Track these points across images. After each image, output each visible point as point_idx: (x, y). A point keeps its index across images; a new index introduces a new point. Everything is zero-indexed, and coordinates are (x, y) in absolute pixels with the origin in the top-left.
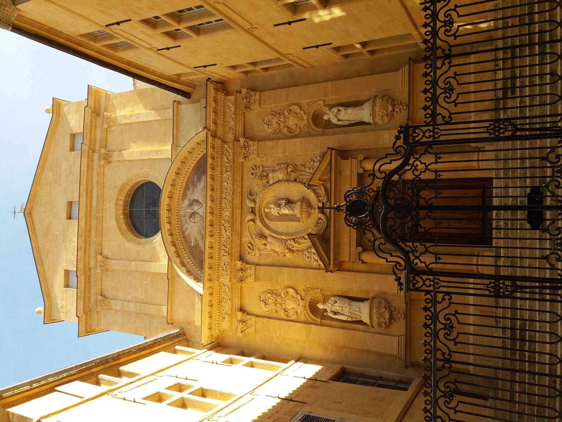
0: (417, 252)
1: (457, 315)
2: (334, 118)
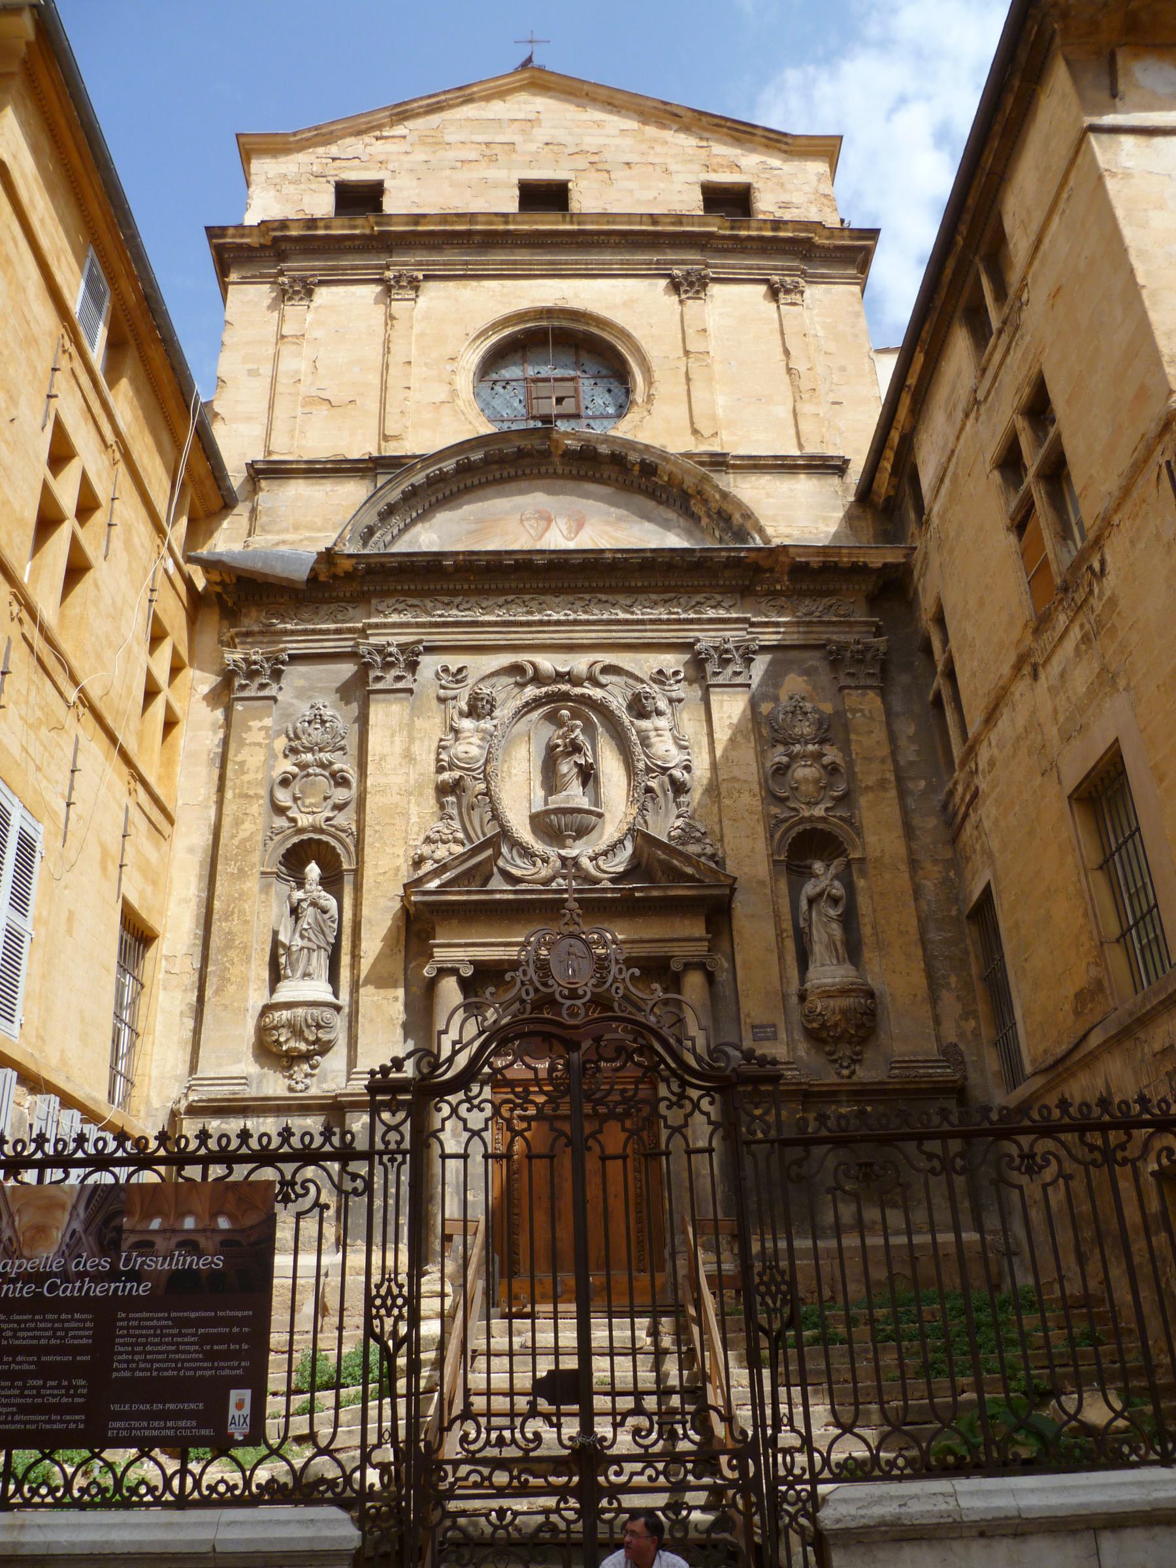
0: (469, 1110)
1: (317, 1210)
2: (818, 889)
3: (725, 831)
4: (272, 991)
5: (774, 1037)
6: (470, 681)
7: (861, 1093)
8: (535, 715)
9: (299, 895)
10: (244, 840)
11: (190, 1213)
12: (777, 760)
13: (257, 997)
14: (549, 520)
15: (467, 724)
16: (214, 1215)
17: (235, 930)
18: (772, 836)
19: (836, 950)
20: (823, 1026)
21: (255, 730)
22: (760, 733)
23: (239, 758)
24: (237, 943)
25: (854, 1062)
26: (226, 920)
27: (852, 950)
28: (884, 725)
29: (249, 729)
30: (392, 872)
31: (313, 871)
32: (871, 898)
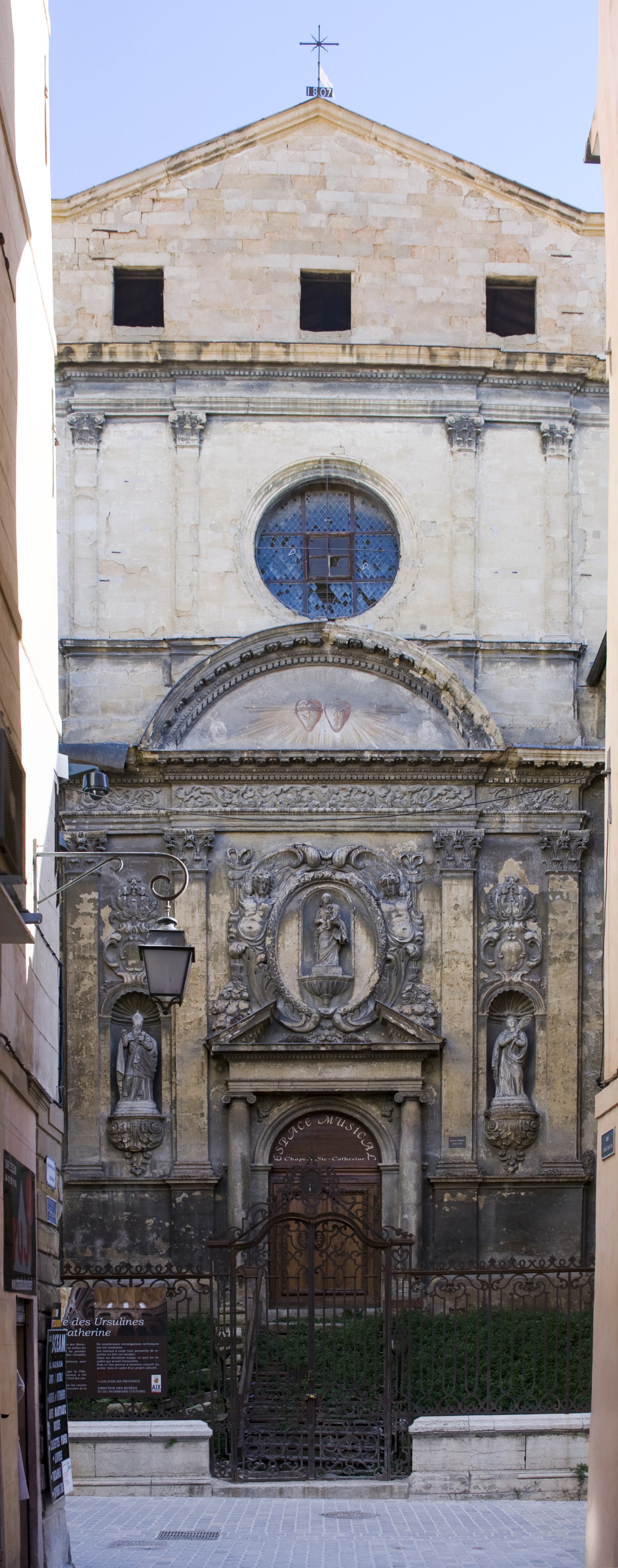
2: (507, 1040)
3: (443, 994)
4: (114, 1107)
5: (464, 1146)
6: (254, 864)
7: (518, 1184)
8: (304, 895)
9: (128, 1037)
10: (85, 994)
11: (126, 1301)
12: (489, 935)
13: (105, 1111)
14: (319, 711)
15: (249, 904)
16: (138, 1302)
17: (84, 1062)
18: (479, 997)
19: (515, 1085)
20: (498, 1138)
21: (85, 901)
22: (479, 910)
23: (75, 926)
24: (87, 1071)
25: (517, 1161)
26: (78, 1055)
27: (527, 1083)
28: (577, 906)
29: (81, 901)
30: (196, 1022)
31: (138, 1019)
32: (547, 1045)
